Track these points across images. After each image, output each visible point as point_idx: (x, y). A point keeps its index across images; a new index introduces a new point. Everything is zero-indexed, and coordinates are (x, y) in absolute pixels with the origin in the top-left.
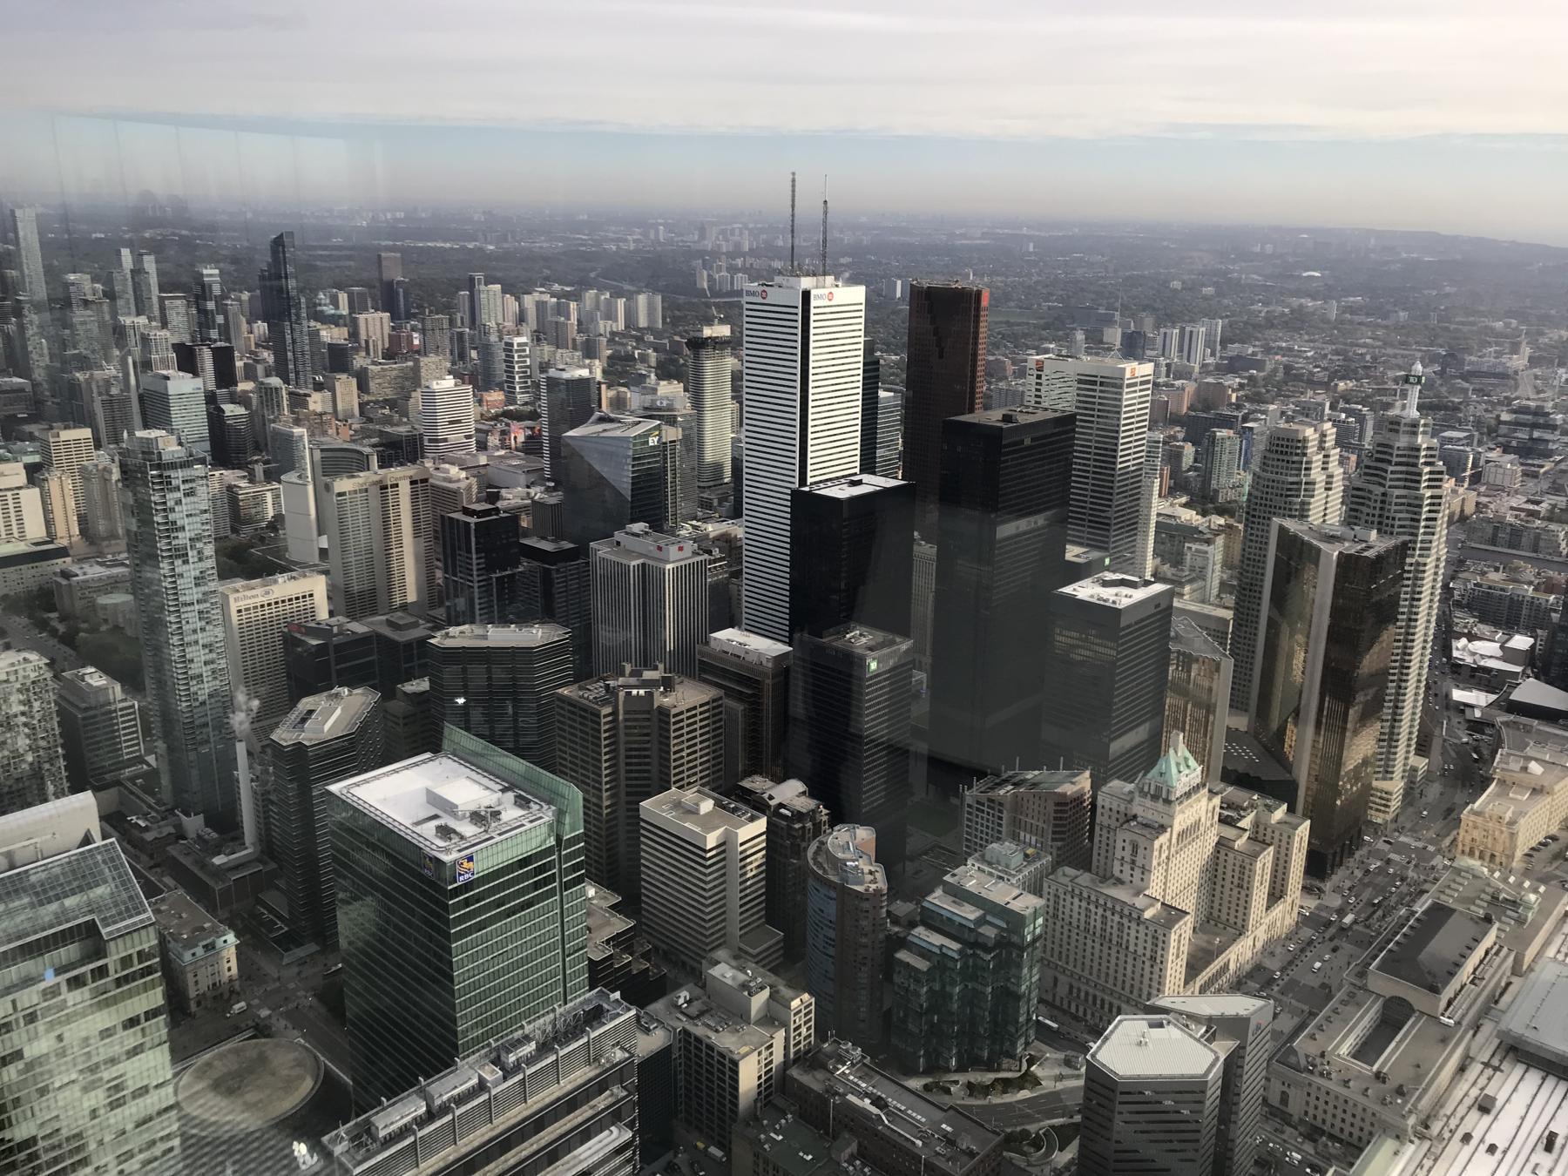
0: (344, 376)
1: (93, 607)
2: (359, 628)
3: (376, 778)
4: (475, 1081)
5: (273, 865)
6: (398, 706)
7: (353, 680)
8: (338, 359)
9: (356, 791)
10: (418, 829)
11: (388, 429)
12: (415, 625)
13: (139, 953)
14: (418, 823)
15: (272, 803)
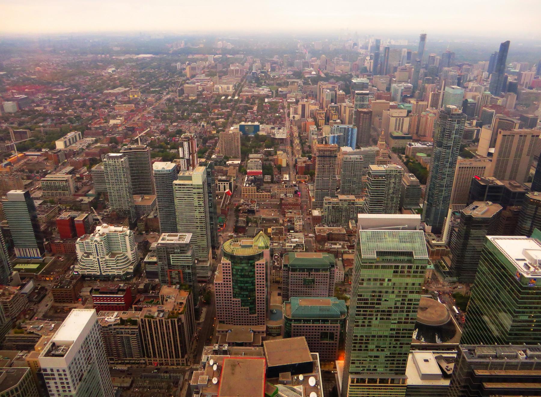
0: (512, 93)
1: (415, 156)
2: (499, 183)
3: (505, 239)
4: (515, 354)
5: (449, 249)
6: (507, 213)
7: (495, 200)
8: (512, 88)
9: (496, 240)
10: (517, 262)
11: (525, 115)
12: (519, 187)
13: (422, 266)
14: (517, 260)
15: (454, 230)
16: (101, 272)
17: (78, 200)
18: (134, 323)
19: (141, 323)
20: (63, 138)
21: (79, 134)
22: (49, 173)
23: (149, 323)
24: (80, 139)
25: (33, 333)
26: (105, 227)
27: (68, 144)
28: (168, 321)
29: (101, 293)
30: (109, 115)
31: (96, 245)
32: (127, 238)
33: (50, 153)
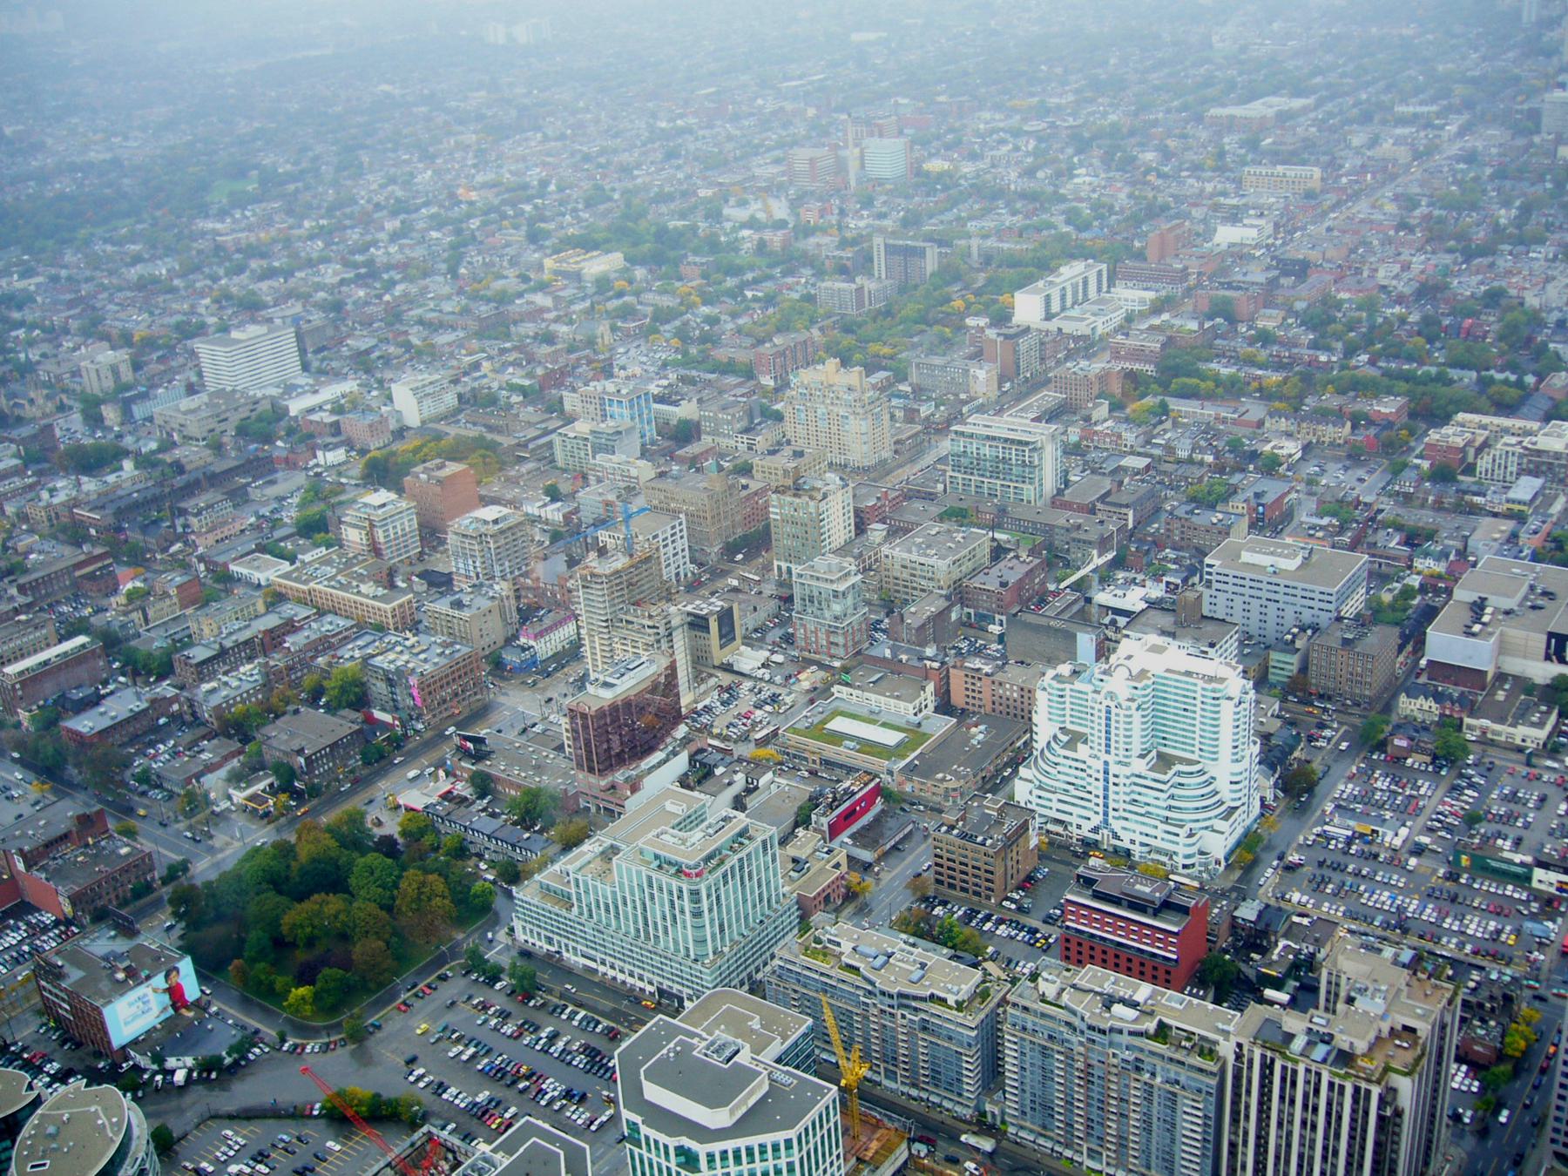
16: (1106, 814)
17: (1062, 522)
18: (1207, 1049)
19: (1231, 1059)
20: (1041, 284)
21: (1100, 273)
22: (981, 409)
23: (1267, 1067)
24: (1099, 290)
25: (854, 969)
26: (1156, 649)
27: (1055, 307)
28: (1342, 1088)
29: (1098, 896)
30: (1216, 207)
31: (1108, 712)
32: (1227, 708)
33: (991, 333)
